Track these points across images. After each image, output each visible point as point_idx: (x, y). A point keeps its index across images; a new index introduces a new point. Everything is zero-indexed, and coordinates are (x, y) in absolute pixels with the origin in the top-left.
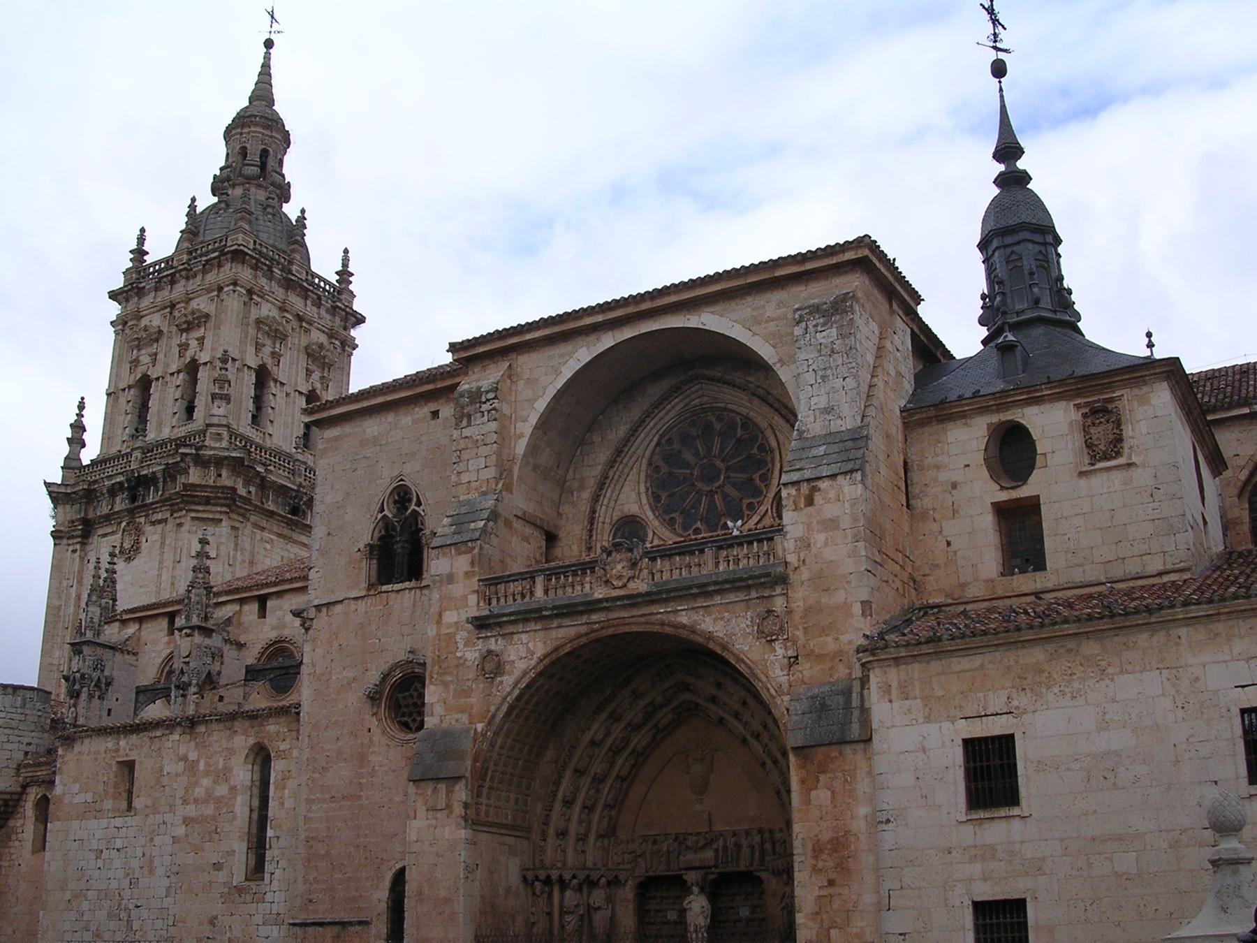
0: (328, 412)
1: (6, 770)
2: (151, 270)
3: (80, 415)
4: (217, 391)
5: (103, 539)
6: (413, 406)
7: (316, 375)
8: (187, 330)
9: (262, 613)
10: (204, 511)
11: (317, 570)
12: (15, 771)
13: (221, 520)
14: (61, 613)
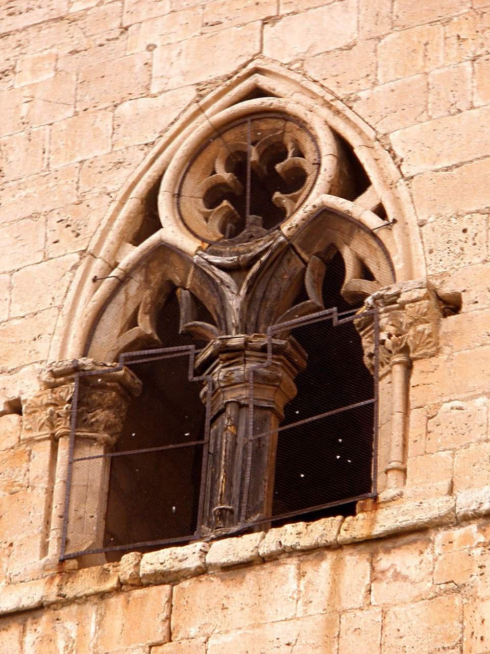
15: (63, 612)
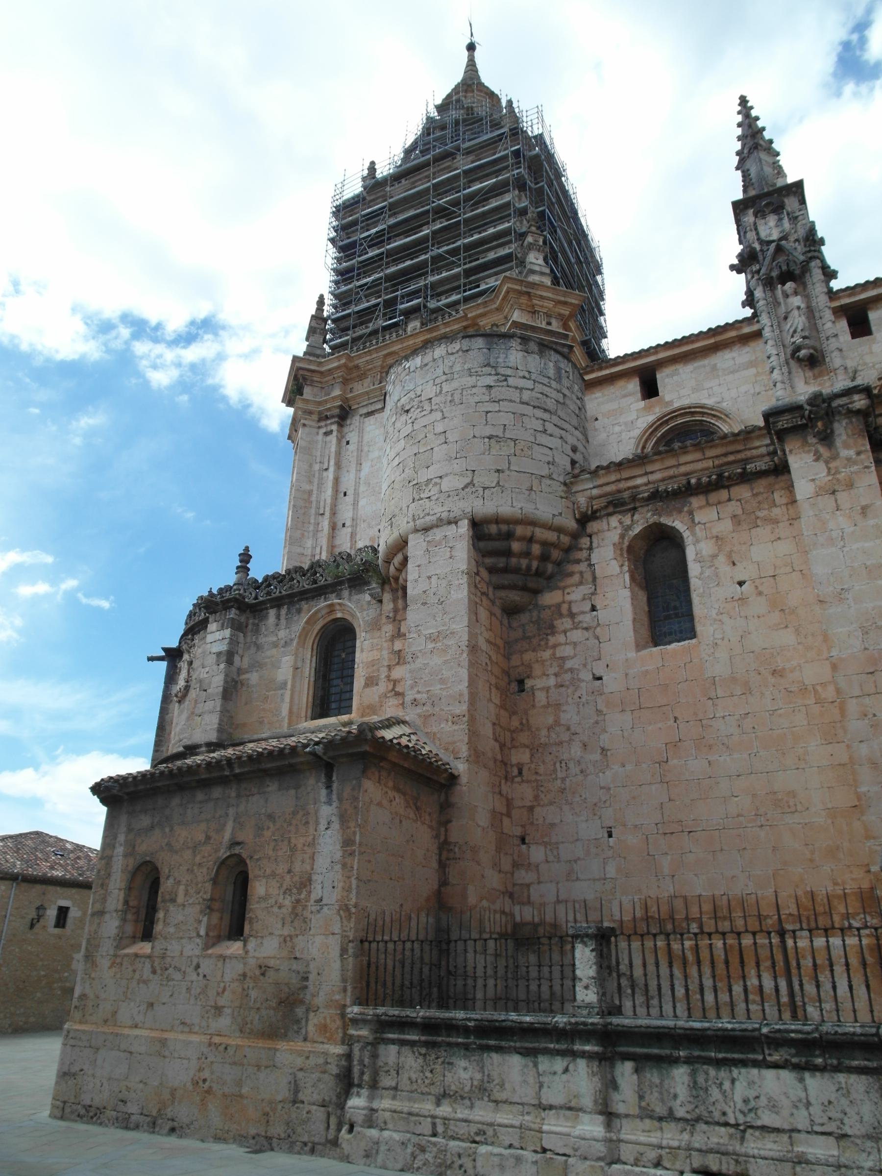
1: (548, 482)
5: (366, 419)
12: (563, 488)
14: (314, 498)
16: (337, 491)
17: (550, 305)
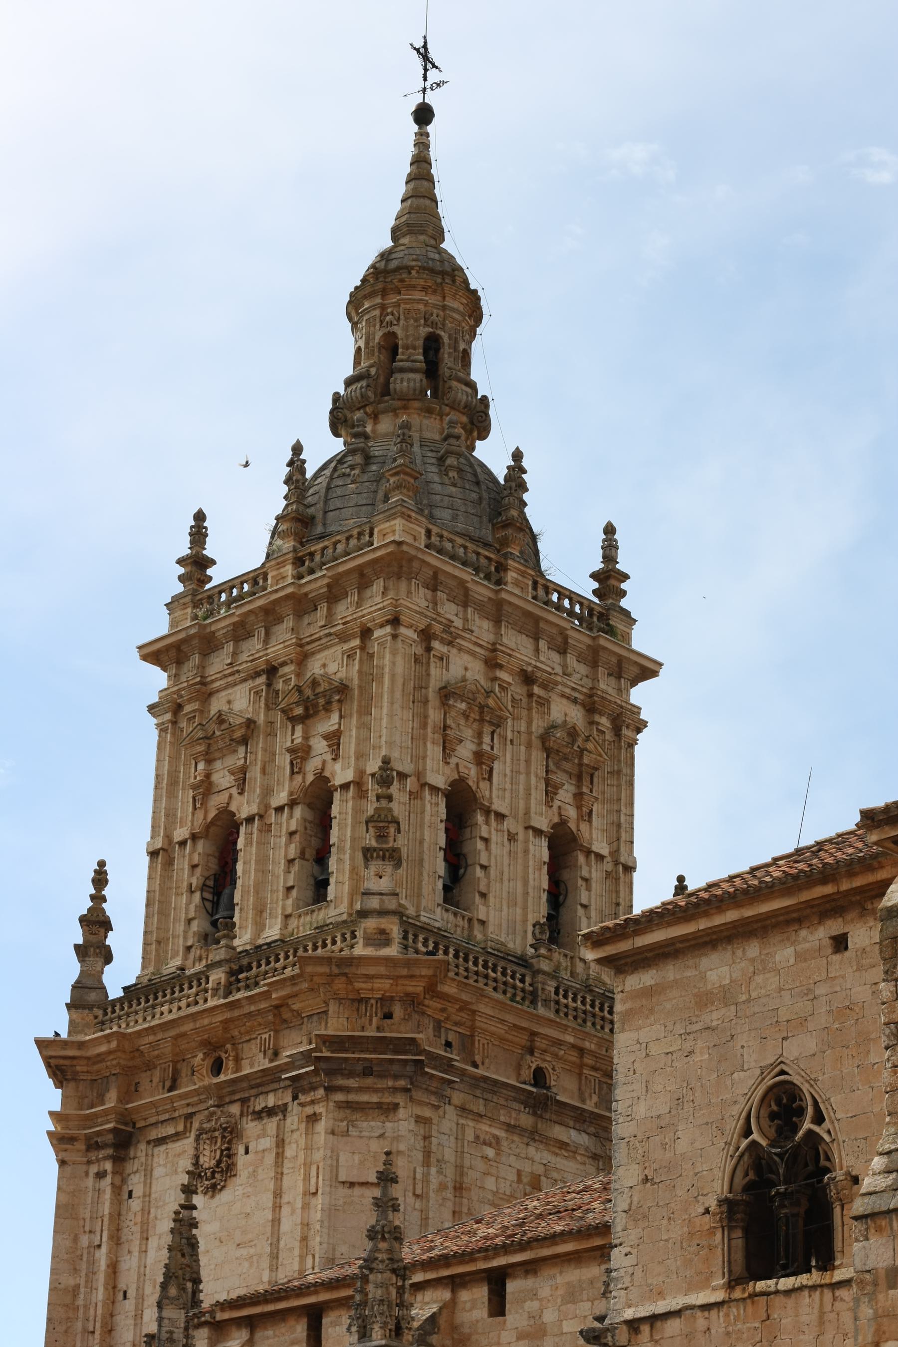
0: (630, 942)
2: (224, 597)
3: (98, 899)
4: (374, 843)
5: (156, 1150)
6: (796, 927)
7: (565, 794)
8: (303, 719)
9: (498, 1307)
10: (360, 1090)
11: (628, 1249)
13: (396, 1106)
14: (80, 1302)
15: (732, 1304)
16: (114, 1287)
17: (386, 984)
